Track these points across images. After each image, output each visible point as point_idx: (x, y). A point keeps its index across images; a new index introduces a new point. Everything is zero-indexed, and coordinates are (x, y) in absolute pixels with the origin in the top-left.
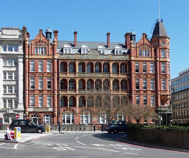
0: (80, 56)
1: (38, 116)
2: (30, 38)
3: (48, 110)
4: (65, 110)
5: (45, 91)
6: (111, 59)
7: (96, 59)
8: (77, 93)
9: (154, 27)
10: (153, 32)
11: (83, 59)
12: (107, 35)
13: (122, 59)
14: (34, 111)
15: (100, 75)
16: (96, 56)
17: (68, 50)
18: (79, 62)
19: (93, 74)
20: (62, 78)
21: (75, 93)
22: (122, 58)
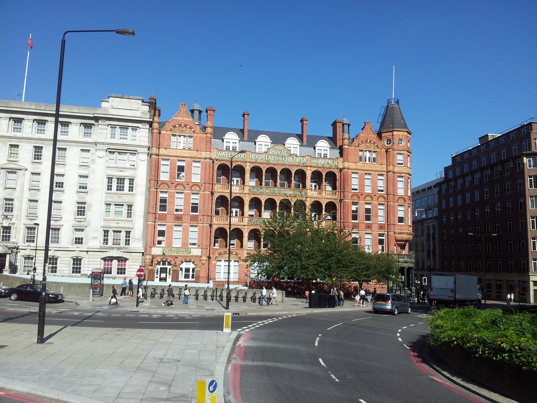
0: (253, 156)
1: (169, 264)
2: (162, 119)
3: (190, 253)
4: (223, 253)
5: (187, 217)
6: (308, 164)
7: (283, 162)
8: (247, 224)
9: (382, 113)
10: (380, 121)
11: (258, 161)
12: (301, 121)
13: (328, 166)
14: (164, 254)
15: (289, 192)
16: (283, 157)
17: (231, 143)
18: (252, 166)
19: (276, 189)
20: (218, 195)
21: (242, 224)
22: (328, 164)
